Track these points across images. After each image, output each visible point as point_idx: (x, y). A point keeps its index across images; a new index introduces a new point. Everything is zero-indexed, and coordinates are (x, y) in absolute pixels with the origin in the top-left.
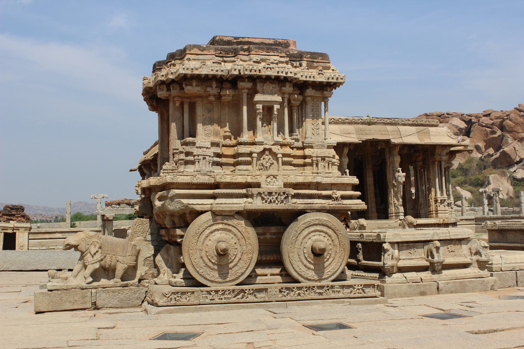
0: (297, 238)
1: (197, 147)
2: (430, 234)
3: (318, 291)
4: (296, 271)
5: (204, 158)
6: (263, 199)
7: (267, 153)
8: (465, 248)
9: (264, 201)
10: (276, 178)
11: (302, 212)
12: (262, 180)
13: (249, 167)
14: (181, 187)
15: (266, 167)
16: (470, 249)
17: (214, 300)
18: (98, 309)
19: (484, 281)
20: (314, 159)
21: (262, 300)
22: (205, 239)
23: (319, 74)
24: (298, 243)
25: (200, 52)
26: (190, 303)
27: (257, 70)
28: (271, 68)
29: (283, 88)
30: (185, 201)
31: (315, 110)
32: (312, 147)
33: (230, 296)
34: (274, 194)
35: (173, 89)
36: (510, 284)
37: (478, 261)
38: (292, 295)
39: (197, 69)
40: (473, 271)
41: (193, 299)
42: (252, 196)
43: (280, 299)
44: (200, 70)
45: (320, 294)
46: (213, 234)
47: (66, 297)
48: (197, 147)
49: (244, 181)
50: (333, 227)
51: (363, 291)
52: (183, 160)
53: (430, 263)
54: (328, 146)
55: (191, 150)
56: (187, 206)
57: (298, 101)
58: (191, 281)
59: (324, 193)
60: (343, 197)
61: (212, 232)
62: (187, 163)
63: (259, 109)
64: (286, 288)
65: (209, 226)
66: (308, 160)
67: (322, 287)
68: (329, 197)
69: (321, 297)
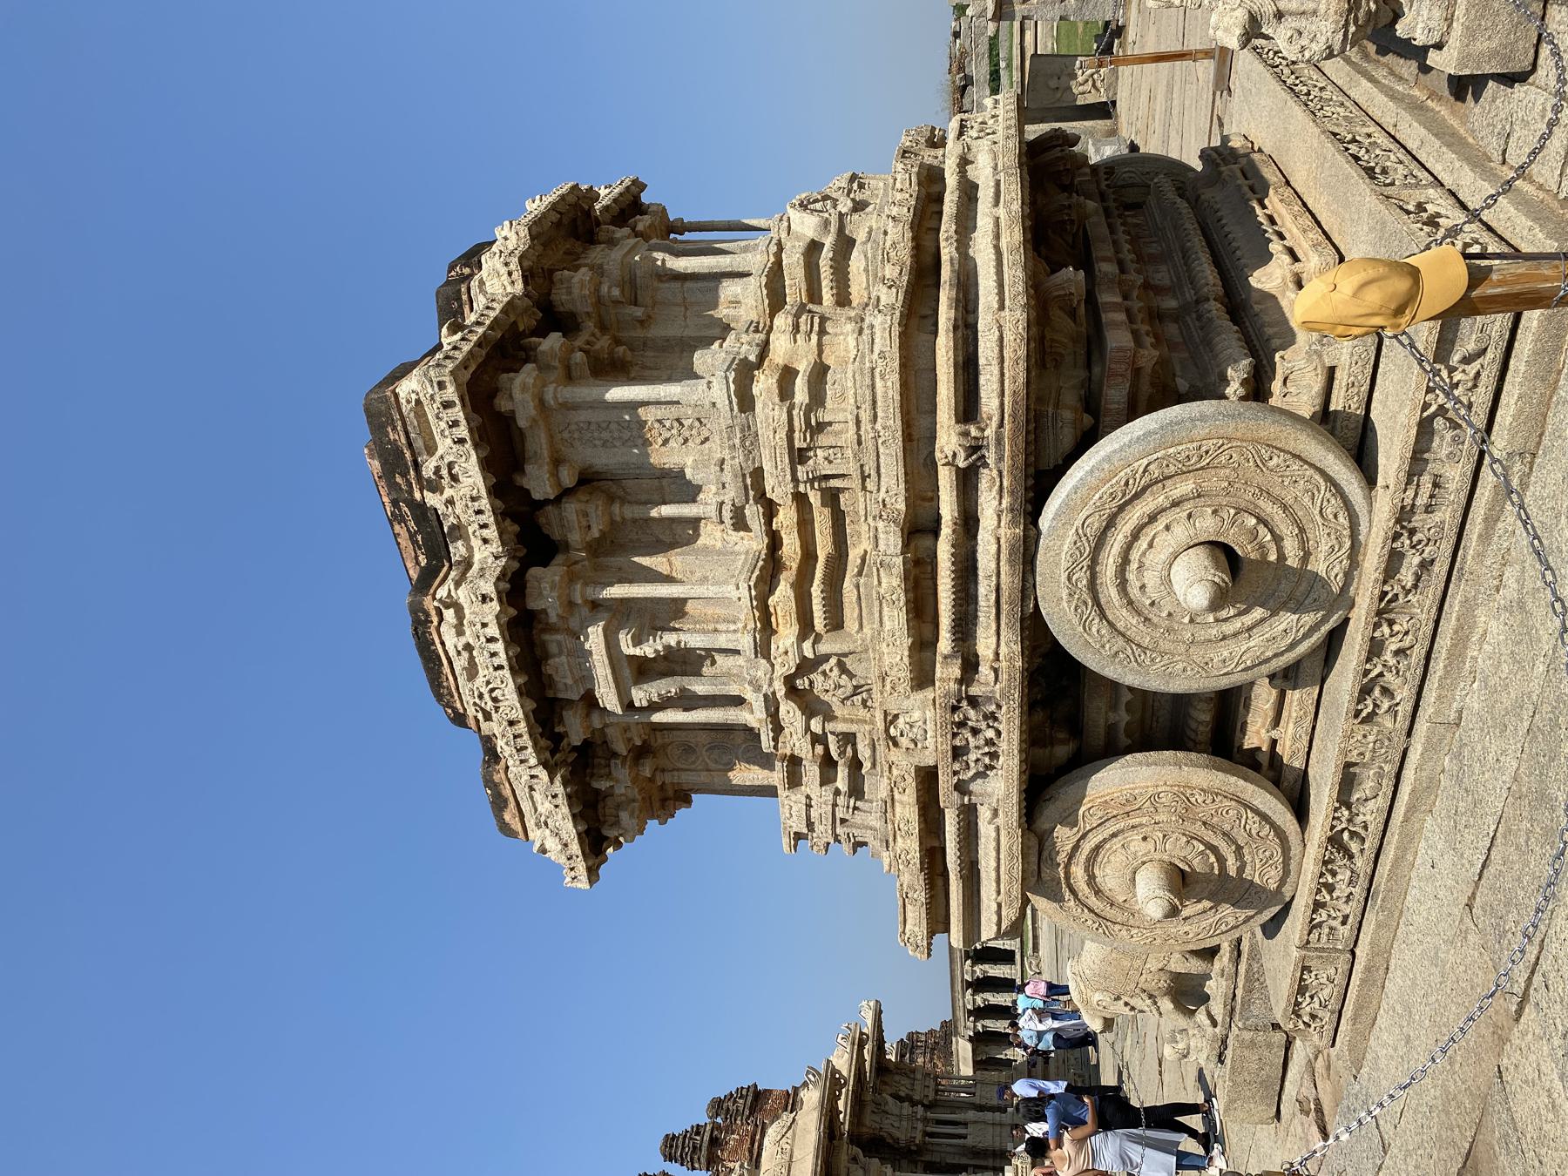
0: (1144, 650)
7: (802, 683)
10: (896, 716)
11: (1034, 630)
12: (904, 763)
14: (943, 912)
23: (454, 478)
25: (512, 804)
26: (1340, 979)
27: (510, 732)
28: (492, 690)
29: (553, 618)
31: (605, 435)
32: (758, 473)
34: (957, 743)
39: (566, 845)
43: (1402, 722)
44: (565, 836)
45: (1426, 565)
54: (742, 410)
57: (586, 515)
59: (948, 508)
60: (968, 409)
64: (1361, 700)
67: (1393, 561)
69: (1440, 569)
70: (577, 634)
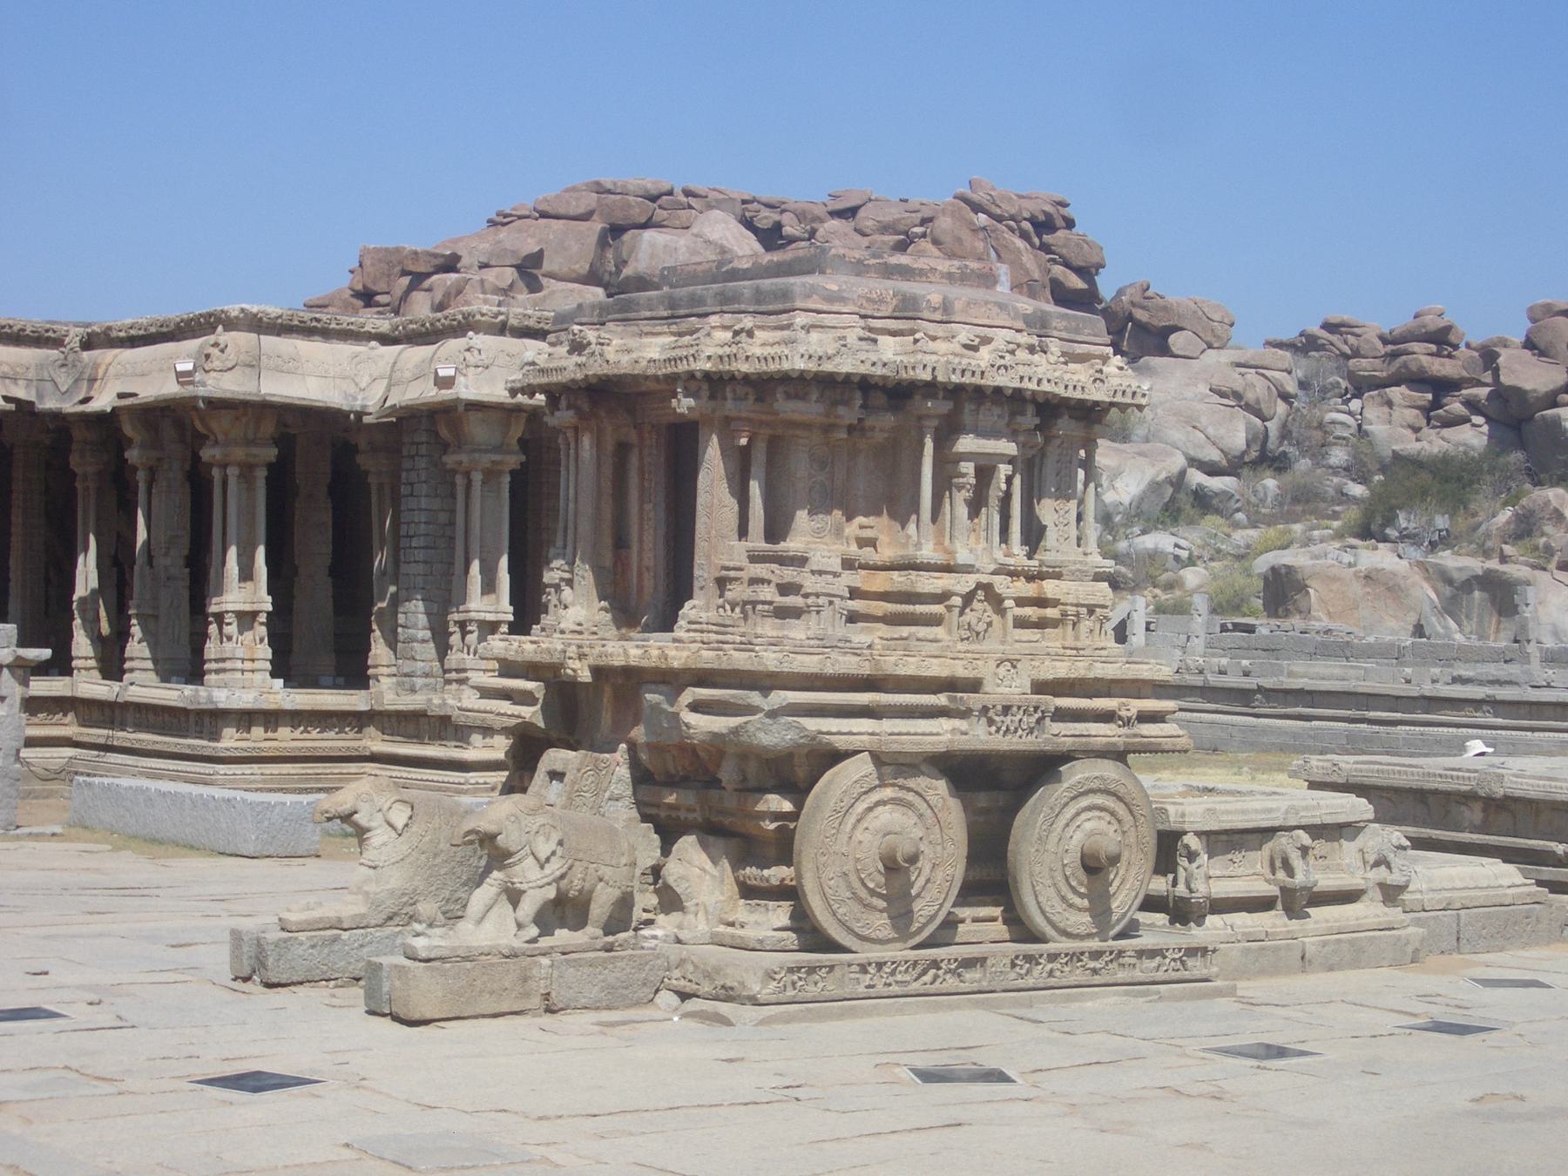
1: (813, 572)
2: (1278, 809)
3: (1092, 964)
4: (1043, 912)
5: (831, 603)
6: (991, 722)
8: (1348, 851)
9: (993, 729)
11: (1067, 757)
12: (985, 670)
13: (939, 632)
15: (978, 634)
16: (1361, 850)
17: (872, 987)
18: (554, 1012)
19: (1399, 938)
20: (1071, 610)
21: (975, 987)
22: (854, 827)
24: (1054, 837)
30: (812, 724)
33: (907, 978)
35: (735, 399)
36: (1444, 946)
37: (1382, 886)
38: (1038, 975)
40: (1368, 911)
41: (830, 986)
42: (964, 714)
44: (837, 360)
45: (1095, 971)
46: (872, 815)
47: (485, 978)
48: (813, 572)
49: (945, 673)
50: (1128, 799)
51: (1183, 963)
52: (770, 603)
53: (1282, 889)
55: (798, 580)
56: (814, 739)
58: (811, 936)
61: (870, 809)
62: (783, 613)
63: (964, 475)
64: (1025, 957)
65: (865, 793)
66: (1051, 613)
68: (1107, 717)
69: (1097, 979)
70: (1013, 435)
